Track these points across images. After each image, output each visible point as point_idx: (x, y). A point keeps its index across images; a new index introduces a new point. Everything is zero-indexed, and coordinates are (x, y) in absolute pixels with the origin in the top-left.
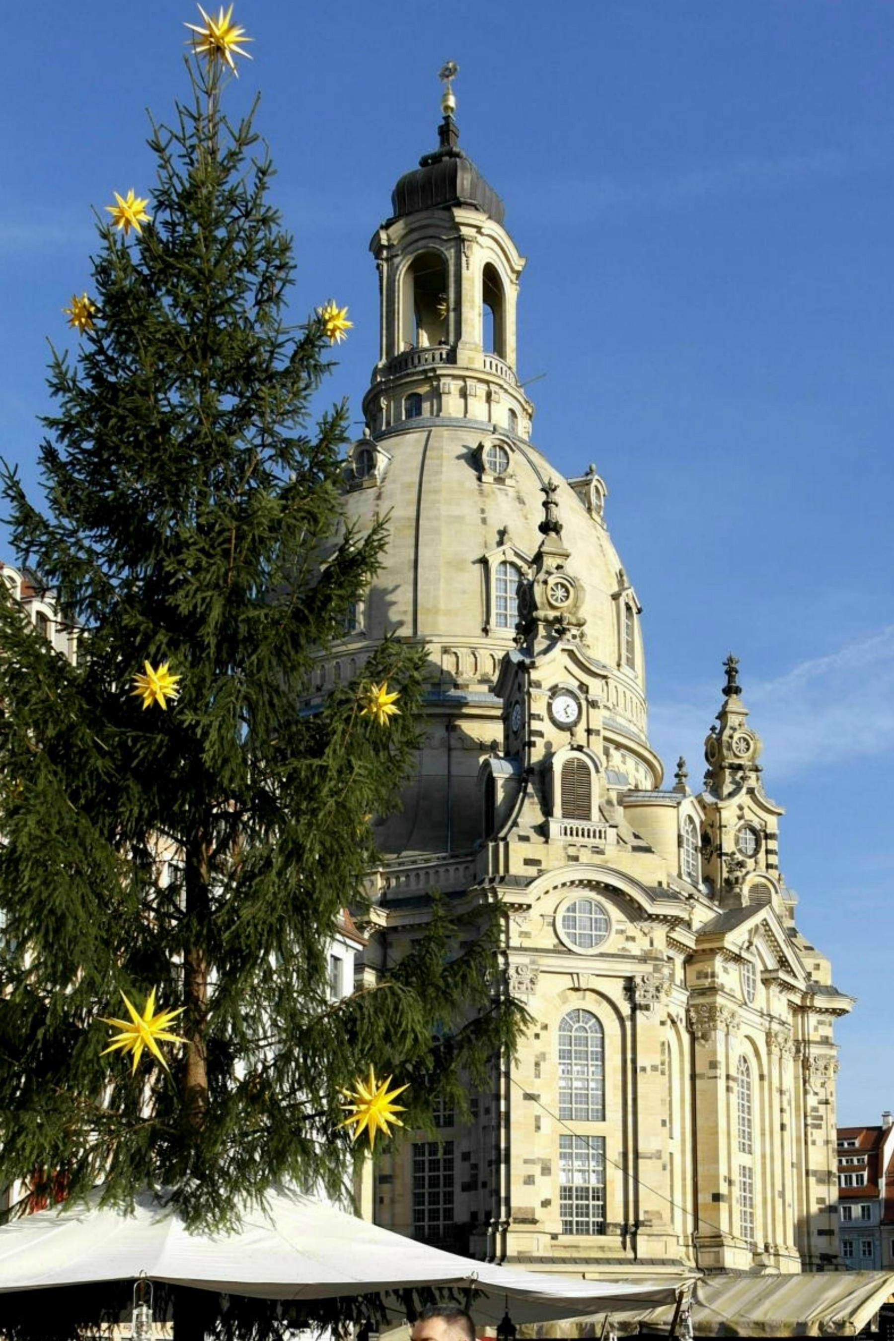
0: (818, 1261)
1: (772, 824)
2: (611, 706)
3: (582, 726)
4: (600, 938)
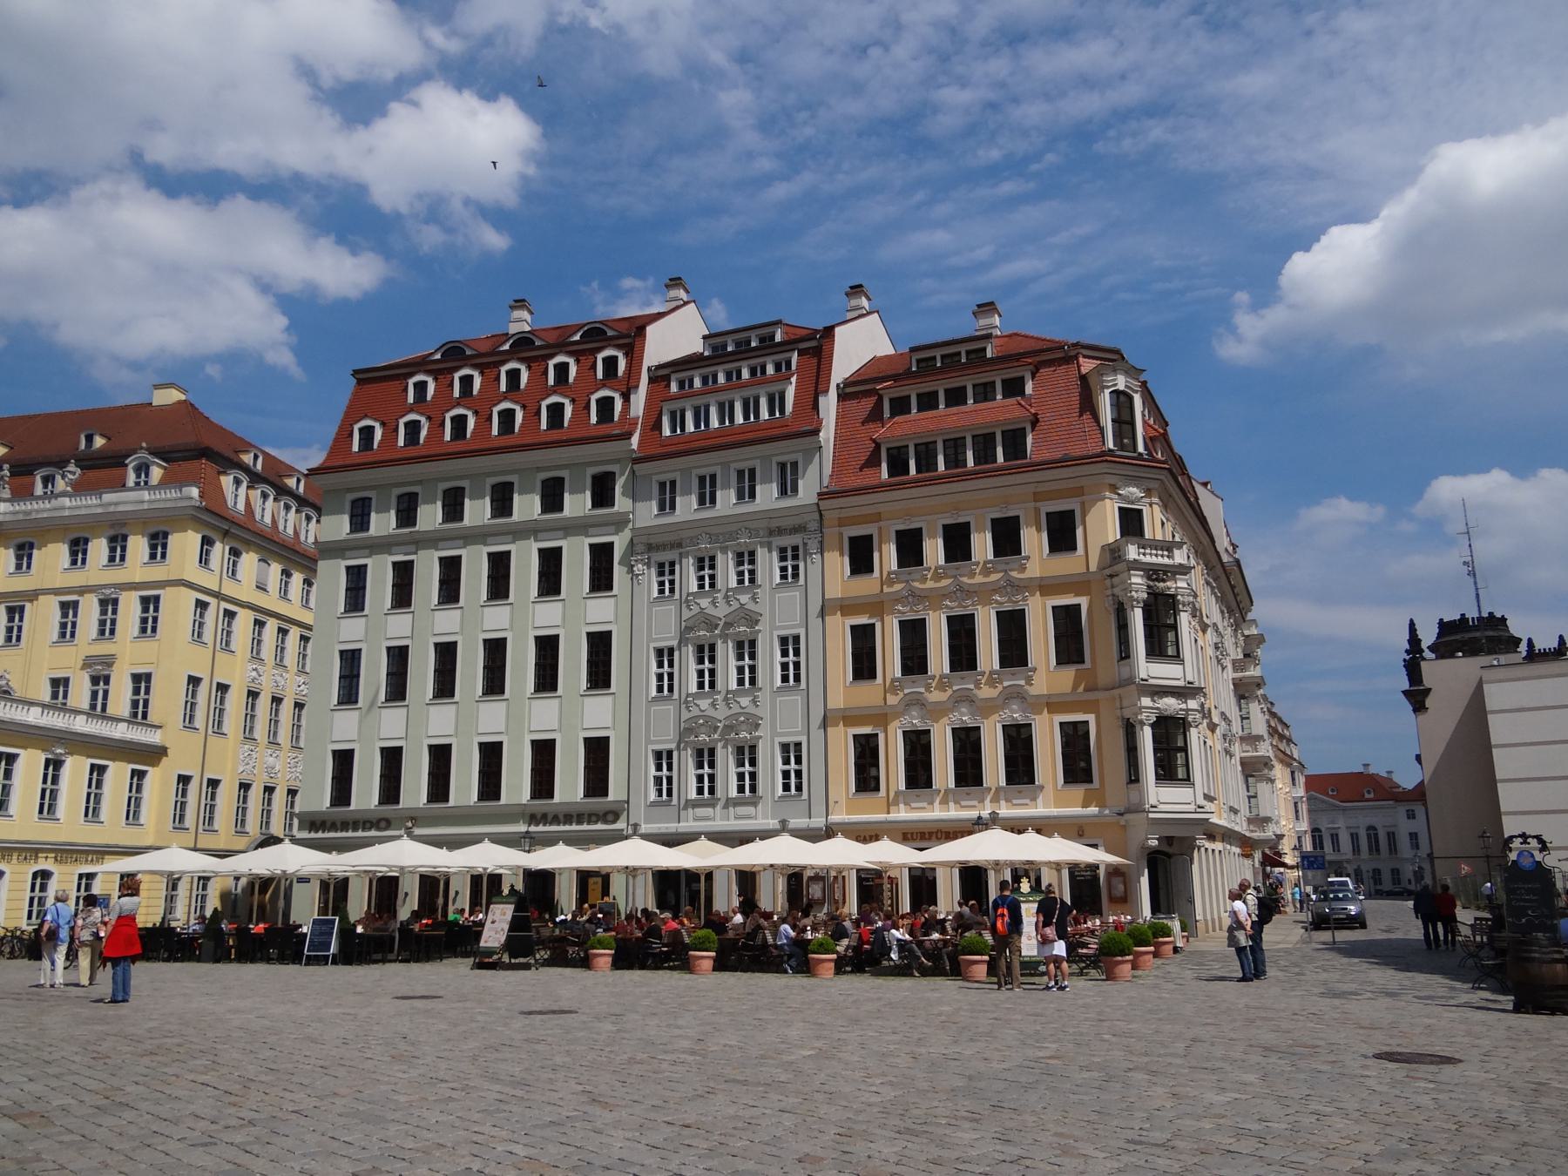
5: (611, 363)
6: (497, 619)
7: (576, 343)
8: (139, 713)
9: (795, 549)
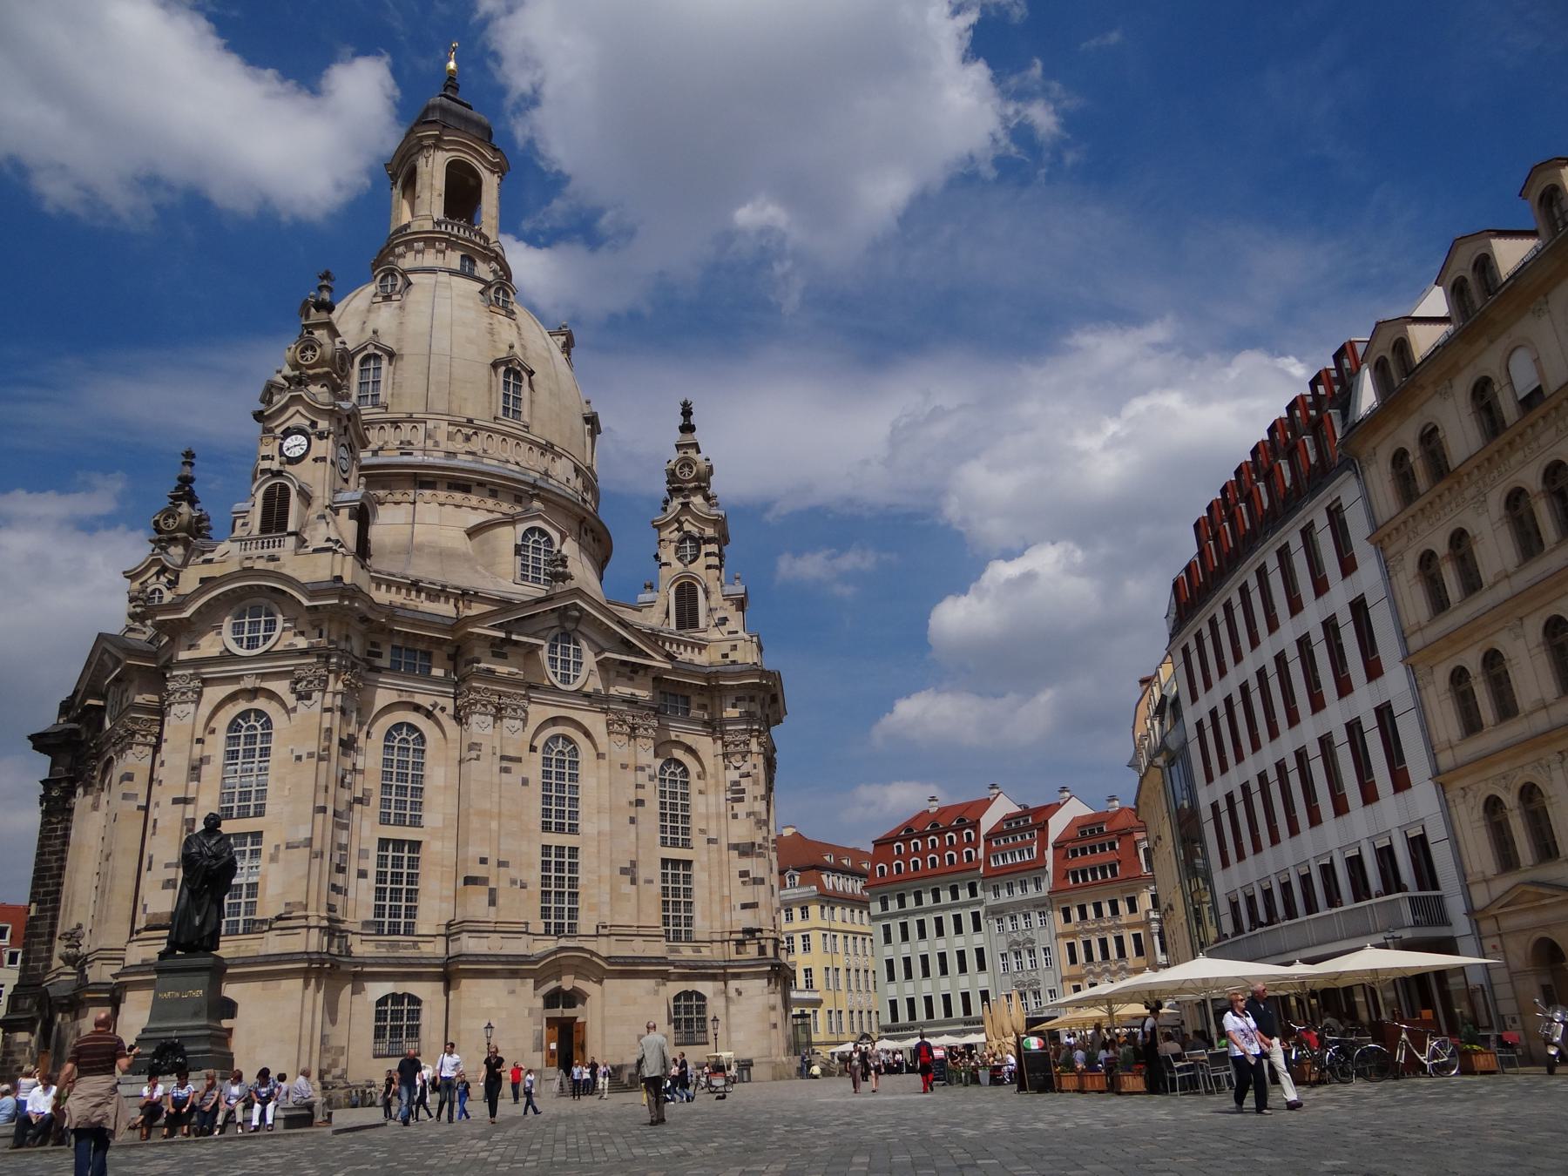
0: (740, 936)
1: (710, 532)
2: (480, 452)
3: (312, 455)
4: (267, 638)
5: (969, 835)
6: (941, 945)
8: (809, 985)
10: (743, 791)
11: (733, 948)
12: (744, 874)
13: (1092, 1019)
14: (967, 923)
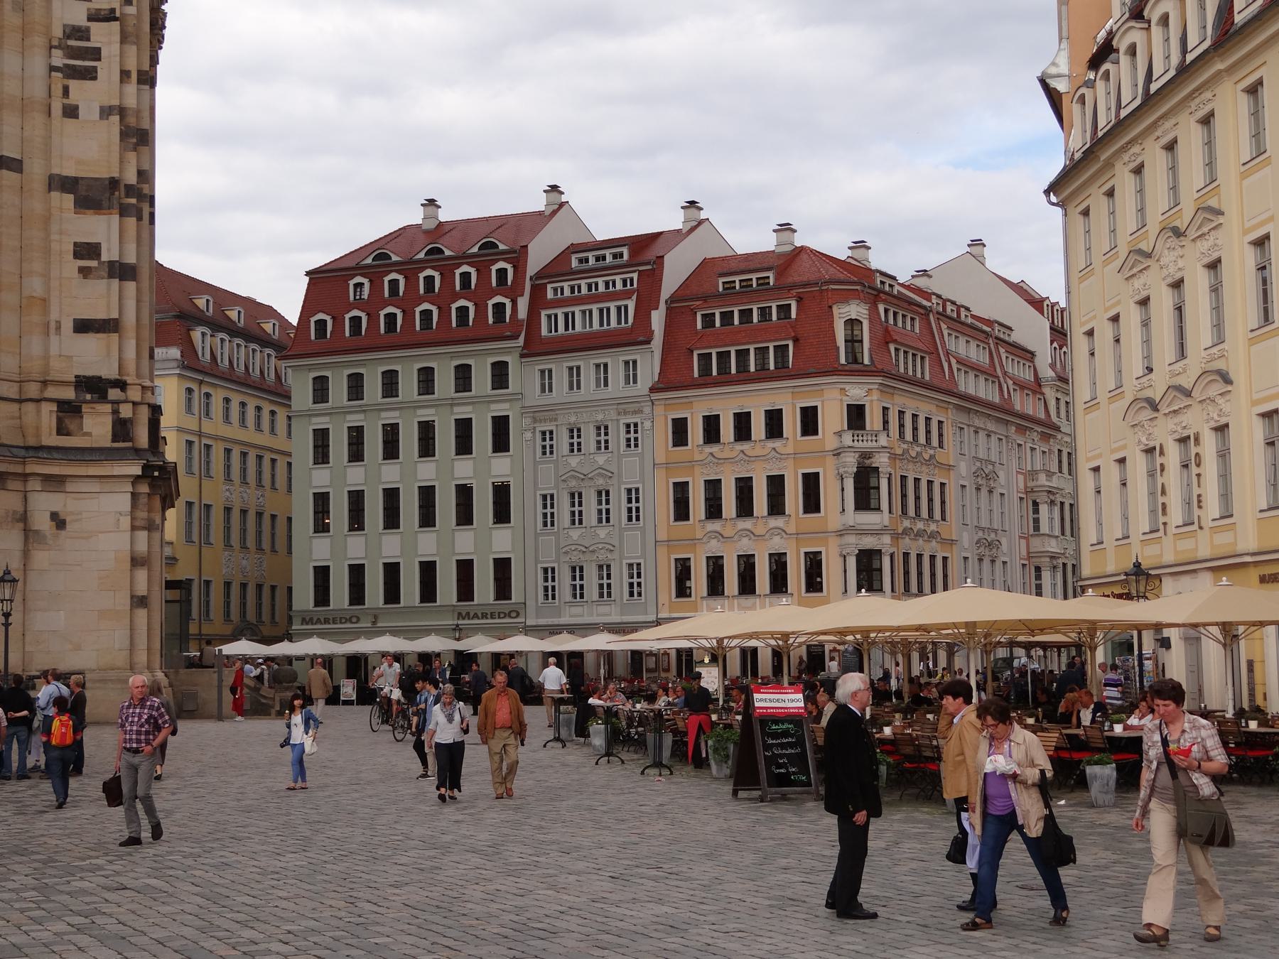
0: (69, 394)
5: (502, 273)
6: (427, 472)
7: (474, 255)
9: (636, 425)
10: (96, 54)
11: (48, 414)
12: (87, 251)
13: (1113, 625)
14: (482, 435)
